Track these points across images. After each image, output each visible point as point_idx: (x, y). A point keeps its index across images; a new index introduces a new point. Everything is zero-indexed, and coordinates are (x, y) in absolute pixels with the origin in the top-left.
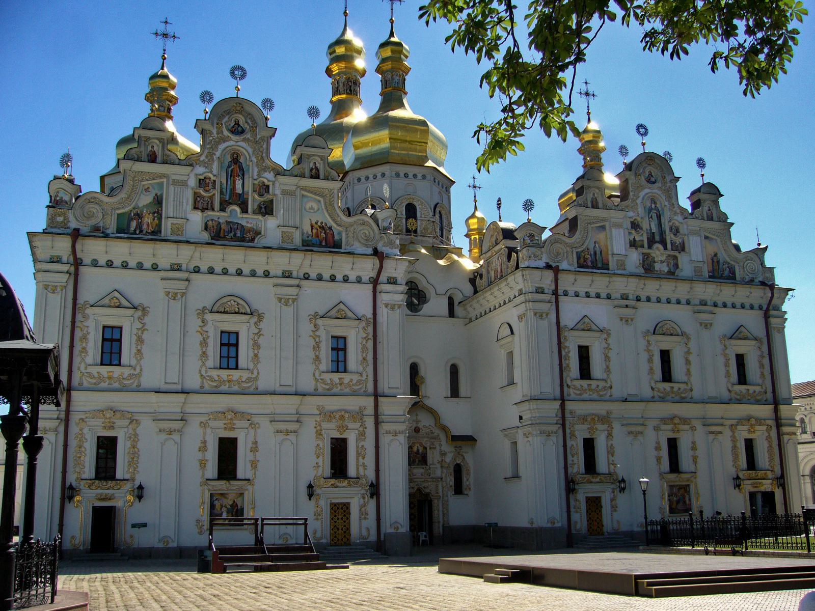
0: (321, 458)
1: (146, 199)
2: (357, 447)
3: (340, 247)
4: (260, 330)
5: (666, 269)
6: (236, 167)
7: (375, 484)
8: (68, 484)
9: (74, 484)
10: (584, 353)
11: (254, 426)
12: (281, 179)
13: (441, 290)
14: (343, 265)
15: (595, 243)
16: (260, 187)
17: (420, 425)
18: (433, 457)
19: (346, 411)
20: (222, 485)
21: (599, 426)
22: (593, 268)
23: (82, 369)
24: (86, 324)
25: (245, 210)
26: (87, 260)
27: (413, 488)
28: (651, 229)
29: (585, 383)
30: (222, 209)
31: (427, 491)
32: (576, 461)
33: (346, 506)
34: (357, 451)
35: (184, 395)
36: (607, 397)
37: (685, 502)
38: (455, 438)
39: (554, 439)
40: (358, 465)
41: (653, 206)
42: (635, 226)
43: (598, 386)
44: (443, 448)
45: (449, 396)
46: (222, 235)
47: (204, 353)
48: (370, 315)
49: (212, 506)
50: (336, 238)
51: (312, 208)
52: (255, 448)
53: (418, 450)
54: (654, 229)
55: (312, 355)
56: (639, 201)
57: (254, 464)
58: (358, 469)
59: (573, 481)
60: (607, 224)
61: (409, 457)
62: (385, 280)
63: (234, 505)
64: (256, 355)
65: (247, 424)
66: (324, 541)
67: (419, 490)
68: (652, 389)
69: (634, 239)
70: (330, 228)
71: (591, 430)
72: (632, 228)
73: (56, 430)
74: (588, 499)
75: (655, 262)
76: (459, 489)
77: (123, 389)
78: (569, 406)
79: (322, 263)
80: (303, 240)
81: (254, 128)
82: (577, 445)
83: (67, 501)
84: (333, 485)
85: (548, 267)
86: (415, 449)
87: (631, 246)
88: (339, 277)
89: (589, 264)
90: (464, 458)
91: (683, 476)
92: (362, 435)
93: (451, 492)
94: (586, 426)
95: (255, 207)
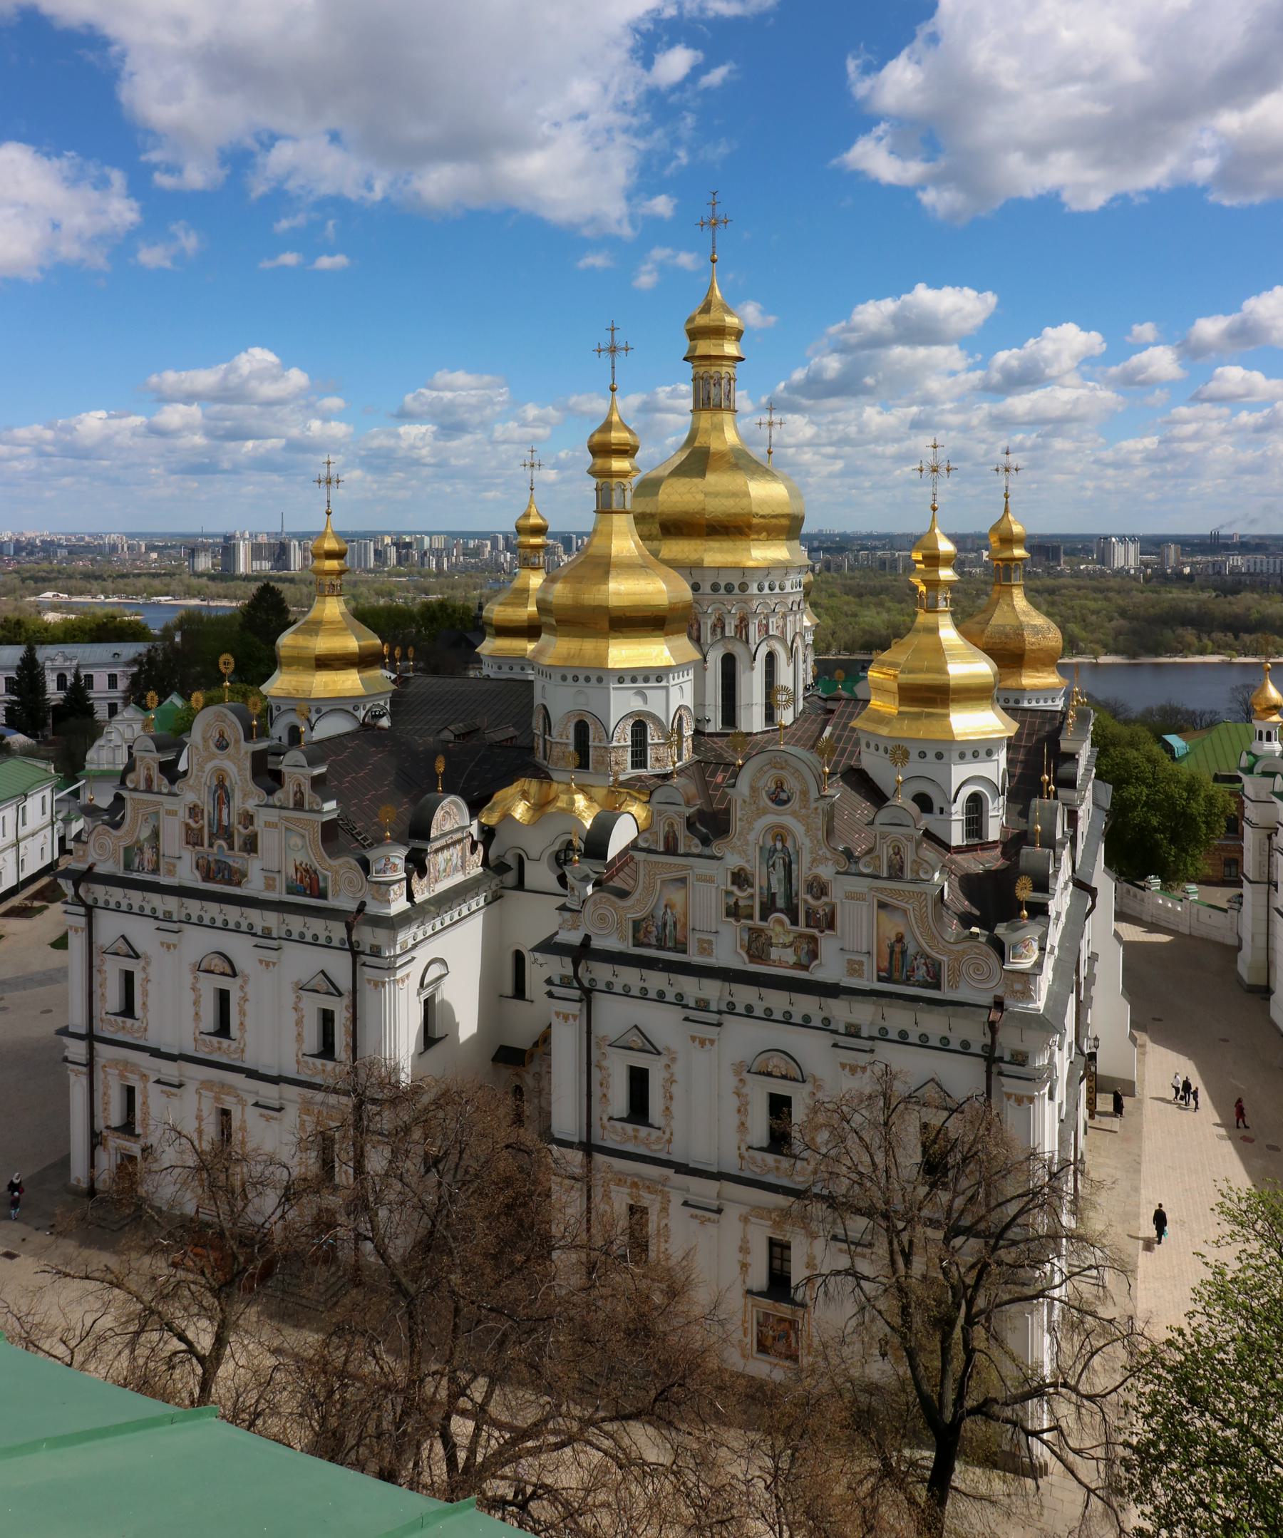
1: (145, 833)
5: (792, 959)
15: (666, 906)
22: (660, 948)
25: (231, 848)
26: (101, 903)
30: (211, 845)
41: (779, 845)
42: (740, 878)
50: (322, 884)
51: (296, 845)
54: (778, 888)
56: (751, 837)
69: (736, 903)
70: (315, 872)
72: (733, 883)
75: (771, 945)
80: (288, 887)
87: (728, 914)
89: (653, 941)
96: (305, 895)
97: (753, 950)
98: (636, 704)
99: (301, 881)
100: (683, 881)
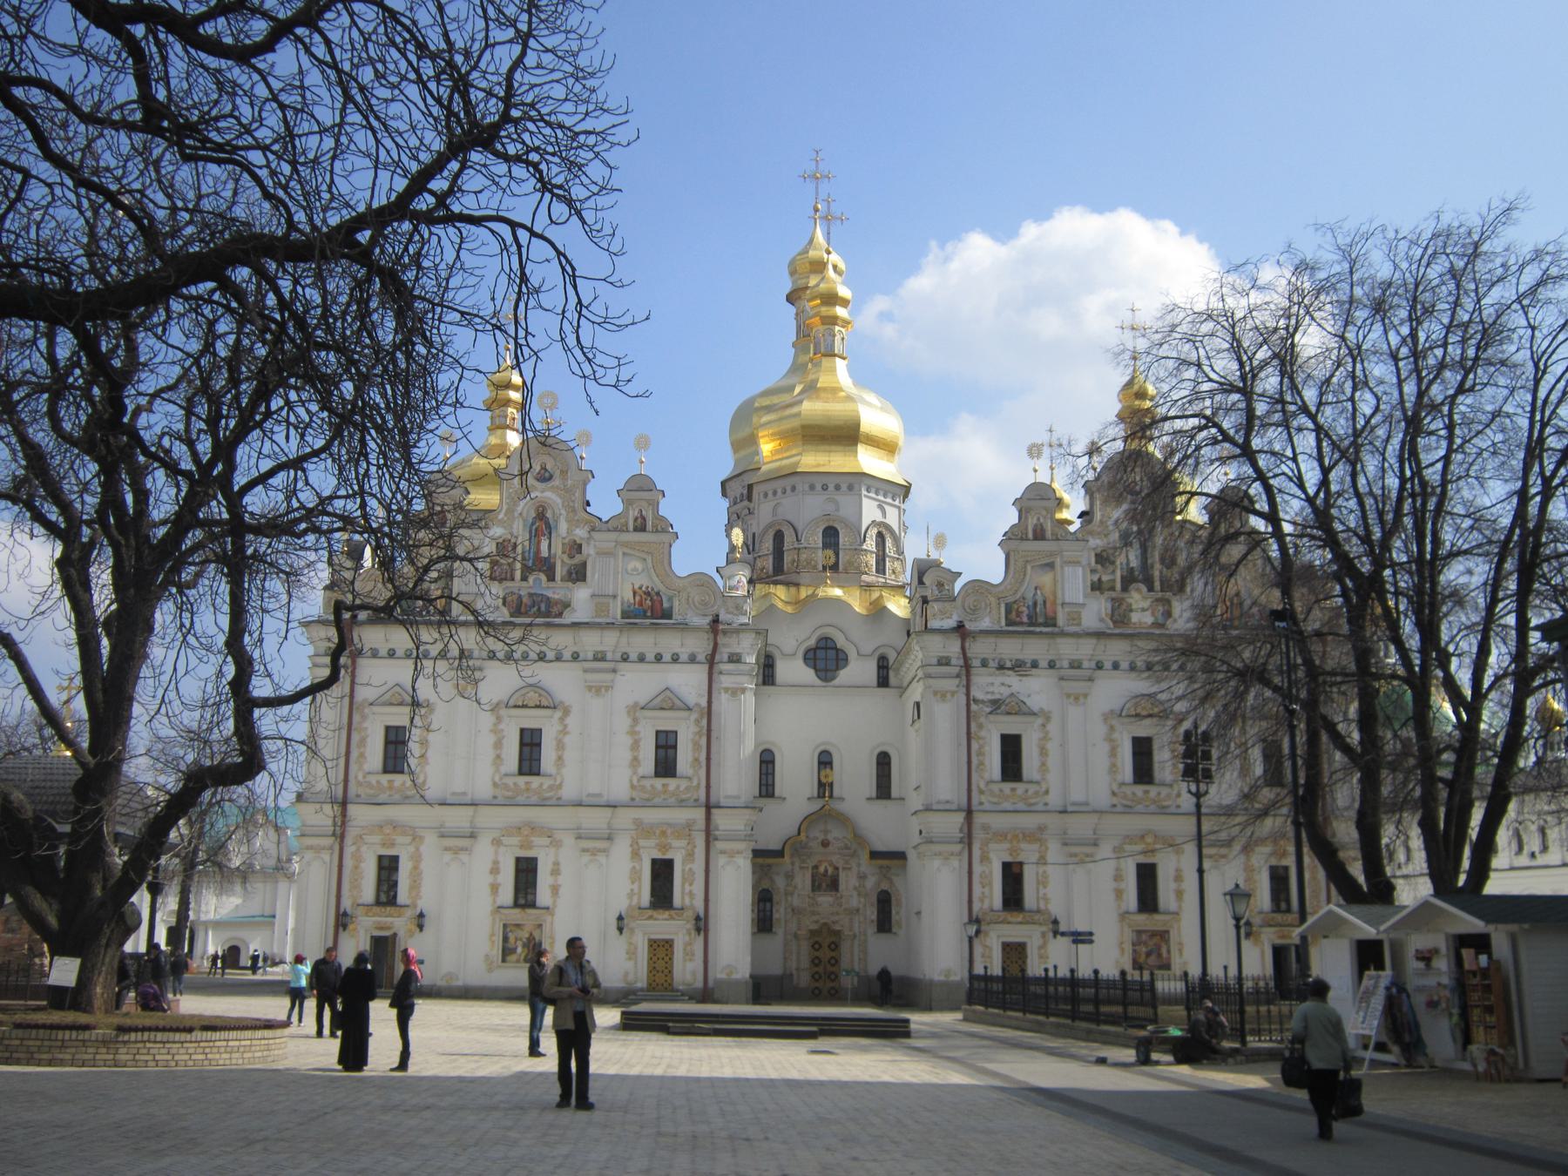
0: (636, 885)
2: (683, 870)
3: (670, 617)
4: (566, 726)
5: (1148, 619)
6: (542, 523)
7: (702, 914)
8: (342, 910)
9: (349, 911)
10: (1011, 747)
11: (557, 844)
12: (596, 535)
13: (868, 648)
14: (670, 642)
16: (571, 548)
17: (830, 837)
18: (848, 881)
19: (669, 825)
20: (516, 915)
21: (1023, 845)
22: (1031, 624)
23: (360, 777)
24: (365, 725)
25: (551, 578)
27: (817, 922)
28: (1128, 564)
29: (1007, 786)
30: (524, 579)
31: (837, 927)
32: (987, 893)
33: (669, 943)
34: (683, 878)
35: (472, 808)
36: (1040, 807)
37: (1160, 955)
38: (875, 855)
39: (955, 863)
40: (683, 893)
42: (1103, 559)
43: (1027, 791)
44: (863, 869)
45: (874, 795)
46: (523, 610)
47: (498, 757)
48: (704, 703)
49: (505, 939)
50: (666, 605)
51: (635, 569)
52: (556, 871)
53: (826, 871)
55: (628, 755)
57: (555, 890)
58: (683, 898)
59: (978, 921)
60: (1058, 561)
61: (813, 881)
62: (725, 658)
63: (531, 938)
64: (560, 758)
65: (546, 841)
66: (639, 985)
67: (825, 924)
68: (1114, 794)
69: (1100, 580)
70: (658, 594)
71: (1012, 851)
72: (1097, 562)
73: (331, 848)
74: (1006, 947)
75: (1131, 611)
76: (884, 923)
77: (405, 800)
78: (979, 819)
79: (643, 642)
81: (564, 473)
82: (991, 873)
83: (341, 929)
84: (651, 917)
85: (960, 627)
86: (822, 869)
87: (1093, 589)
88: (667, 657)
89: (1025, 619)
90: (891, 882)
91: (1157, 917)
92: (690, 856)
93: (872, 929)
94: (1006, 845)
95: (564, 573)
96: (645, 617)
97: (1116, 617)
98: (879, 518)
99: (641, 604)
100: (1051, 566)
